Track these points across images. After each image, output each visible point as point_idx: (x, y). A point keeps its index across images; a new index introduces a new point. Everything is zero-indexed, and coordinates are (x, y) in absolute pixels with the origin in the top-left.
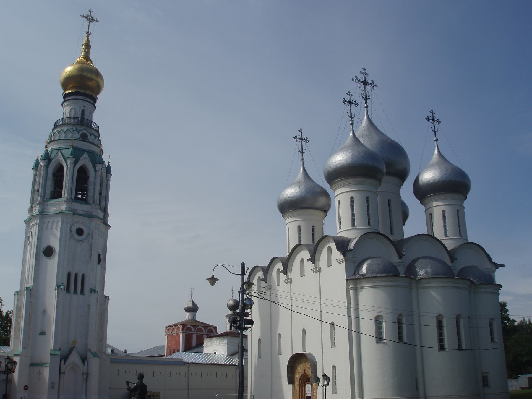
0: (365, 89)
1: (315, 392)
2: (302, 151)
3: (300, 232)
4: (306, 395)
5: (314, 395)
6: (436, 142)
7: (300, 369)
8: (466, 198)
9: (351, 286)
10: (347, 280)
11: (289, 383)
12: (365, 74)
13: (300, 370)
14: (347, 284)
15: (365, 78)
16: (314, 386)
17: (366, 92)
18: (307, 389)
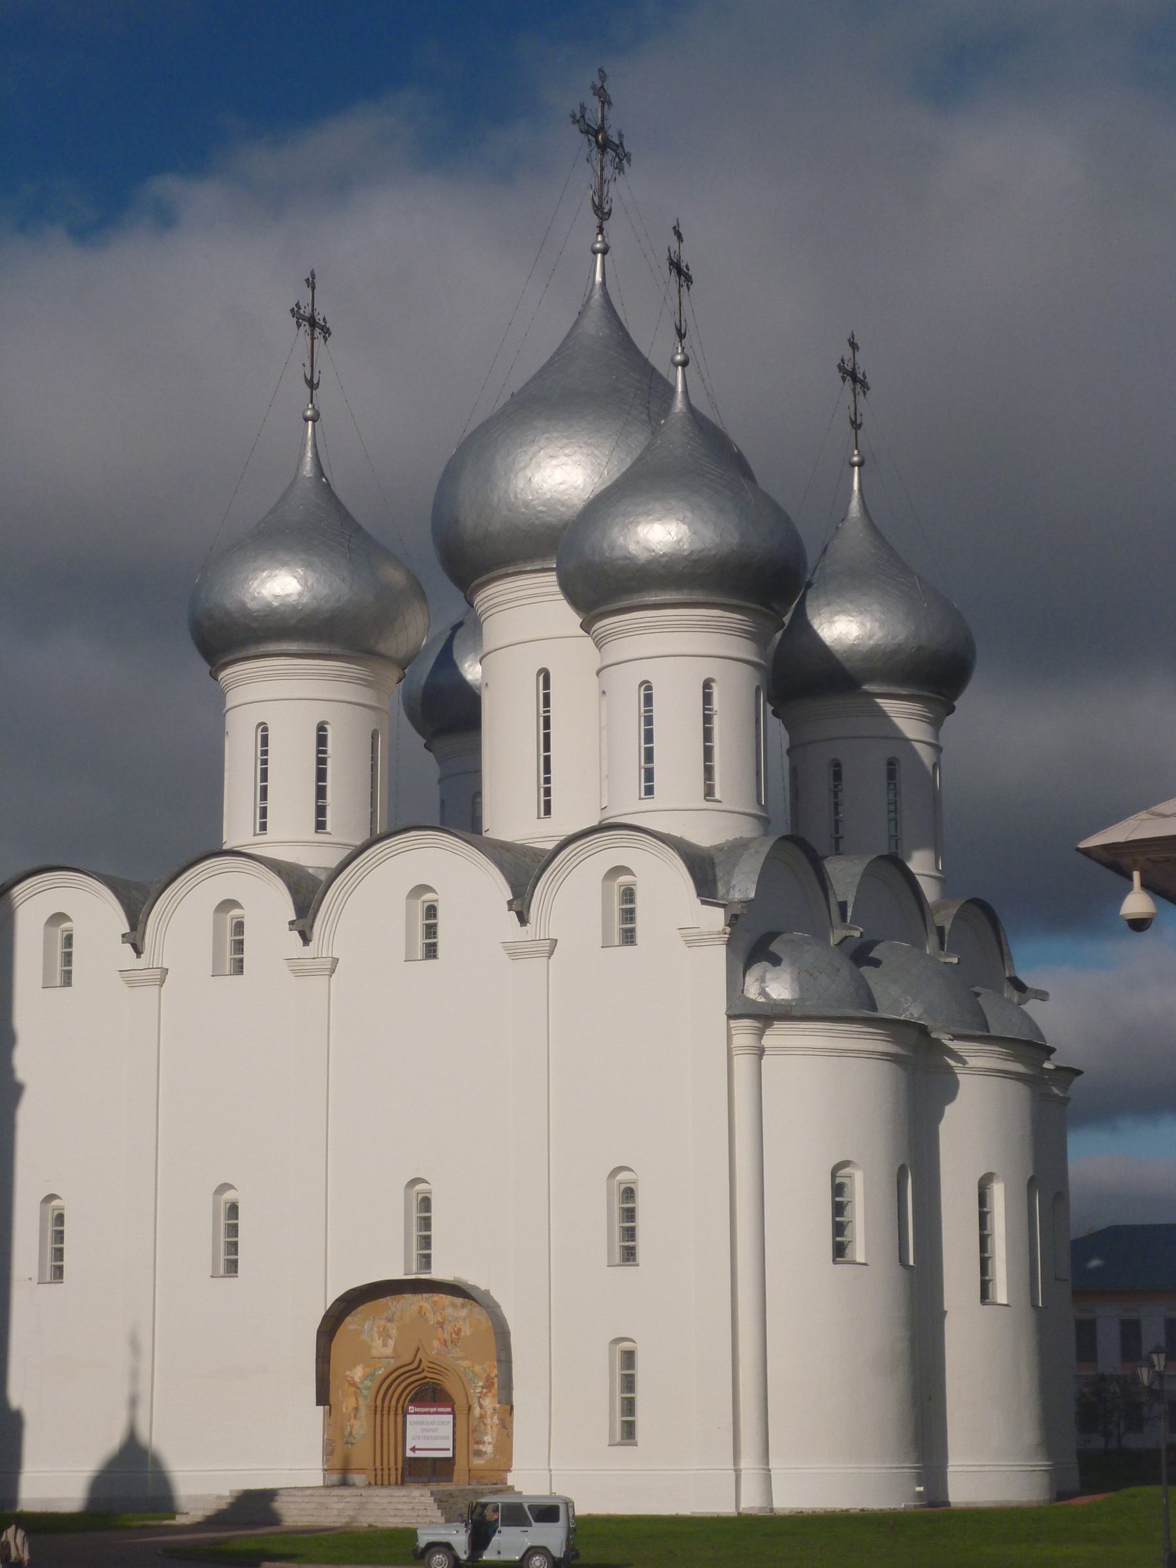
1: (487, 1439)
2: (312, 377)
3: (325, 752)
4: (409, 1454)
5: (479, 1453)
6: (856, 468)
11: (317, 1405)
12: (605, 101)
16: (482, 1417)
18: (411, 1431)
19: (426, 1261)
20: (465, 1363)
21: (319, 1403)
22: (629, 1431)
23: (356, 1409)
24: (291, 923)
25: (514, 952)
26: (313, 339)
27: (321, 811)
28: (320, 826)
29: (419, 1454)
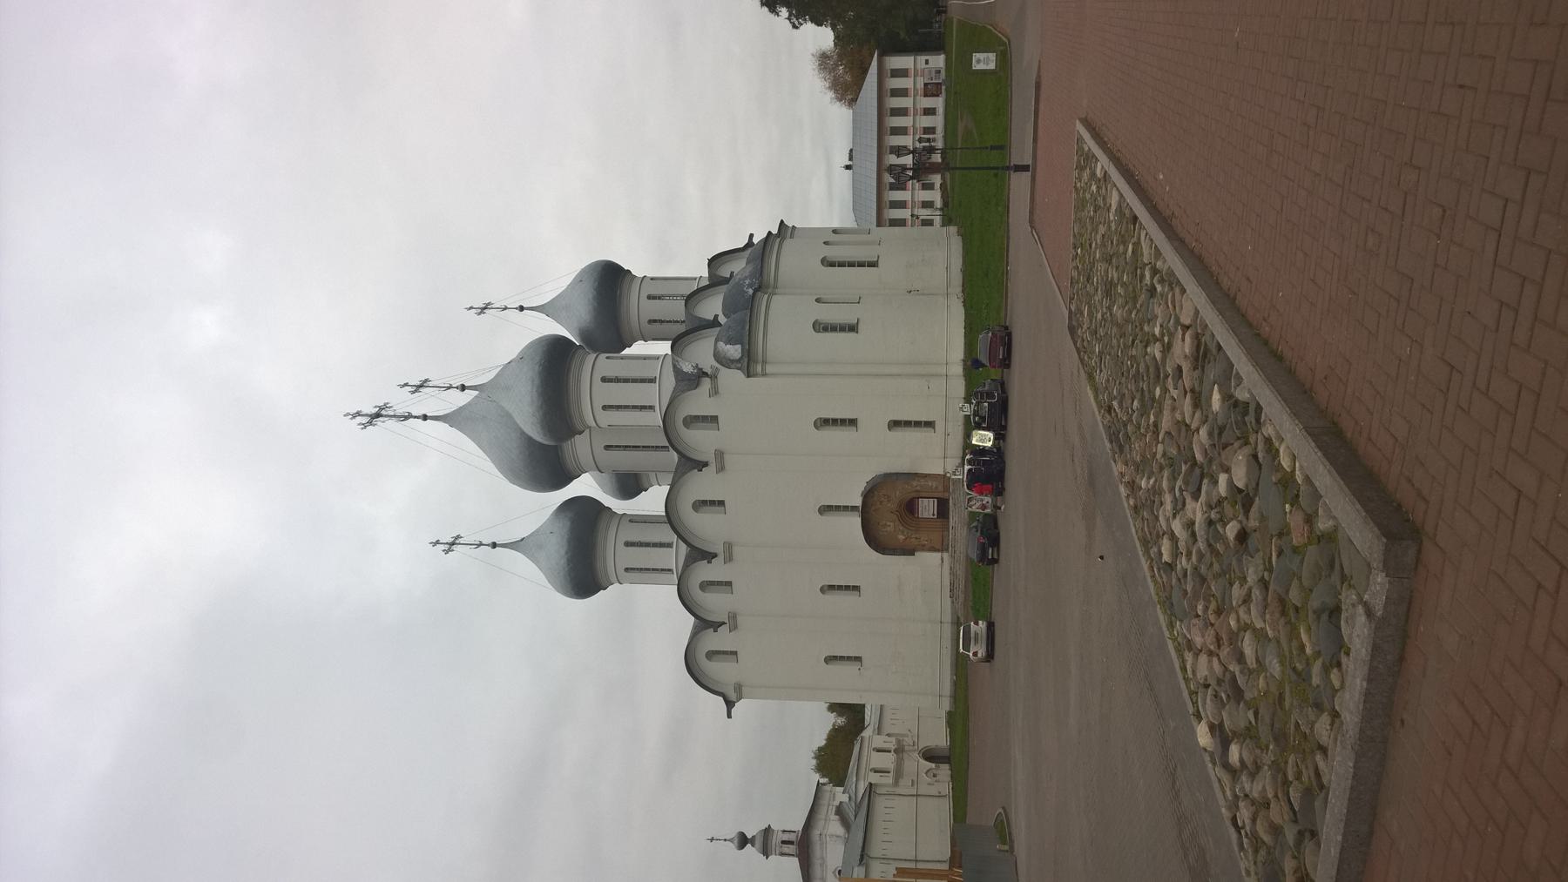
0: (386, 416)
1: (930, 484)
5: (936, 488)
7: (889, 526)
8: (629, 271)
9: (759, 368)
10: (749, 376)
12: (358, 414)
13: (890, 527)
14: (755, 375)
15: (367, 415)
17: (394, 416)
18: (926, 515)
19: (854, 508)
20: (898, 493)
21: (914, 555)
22: (930, 424)
23: (916, 538)
24: (708, 562)
25: (721, 468)
26: (460, 544)
27: (662, 545)
28: (669, 545)
29: (936, 513)
